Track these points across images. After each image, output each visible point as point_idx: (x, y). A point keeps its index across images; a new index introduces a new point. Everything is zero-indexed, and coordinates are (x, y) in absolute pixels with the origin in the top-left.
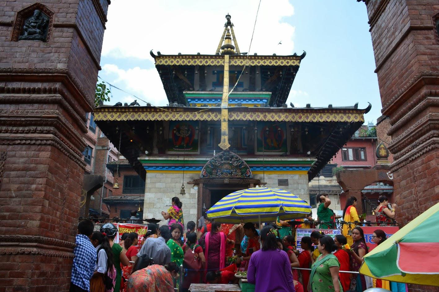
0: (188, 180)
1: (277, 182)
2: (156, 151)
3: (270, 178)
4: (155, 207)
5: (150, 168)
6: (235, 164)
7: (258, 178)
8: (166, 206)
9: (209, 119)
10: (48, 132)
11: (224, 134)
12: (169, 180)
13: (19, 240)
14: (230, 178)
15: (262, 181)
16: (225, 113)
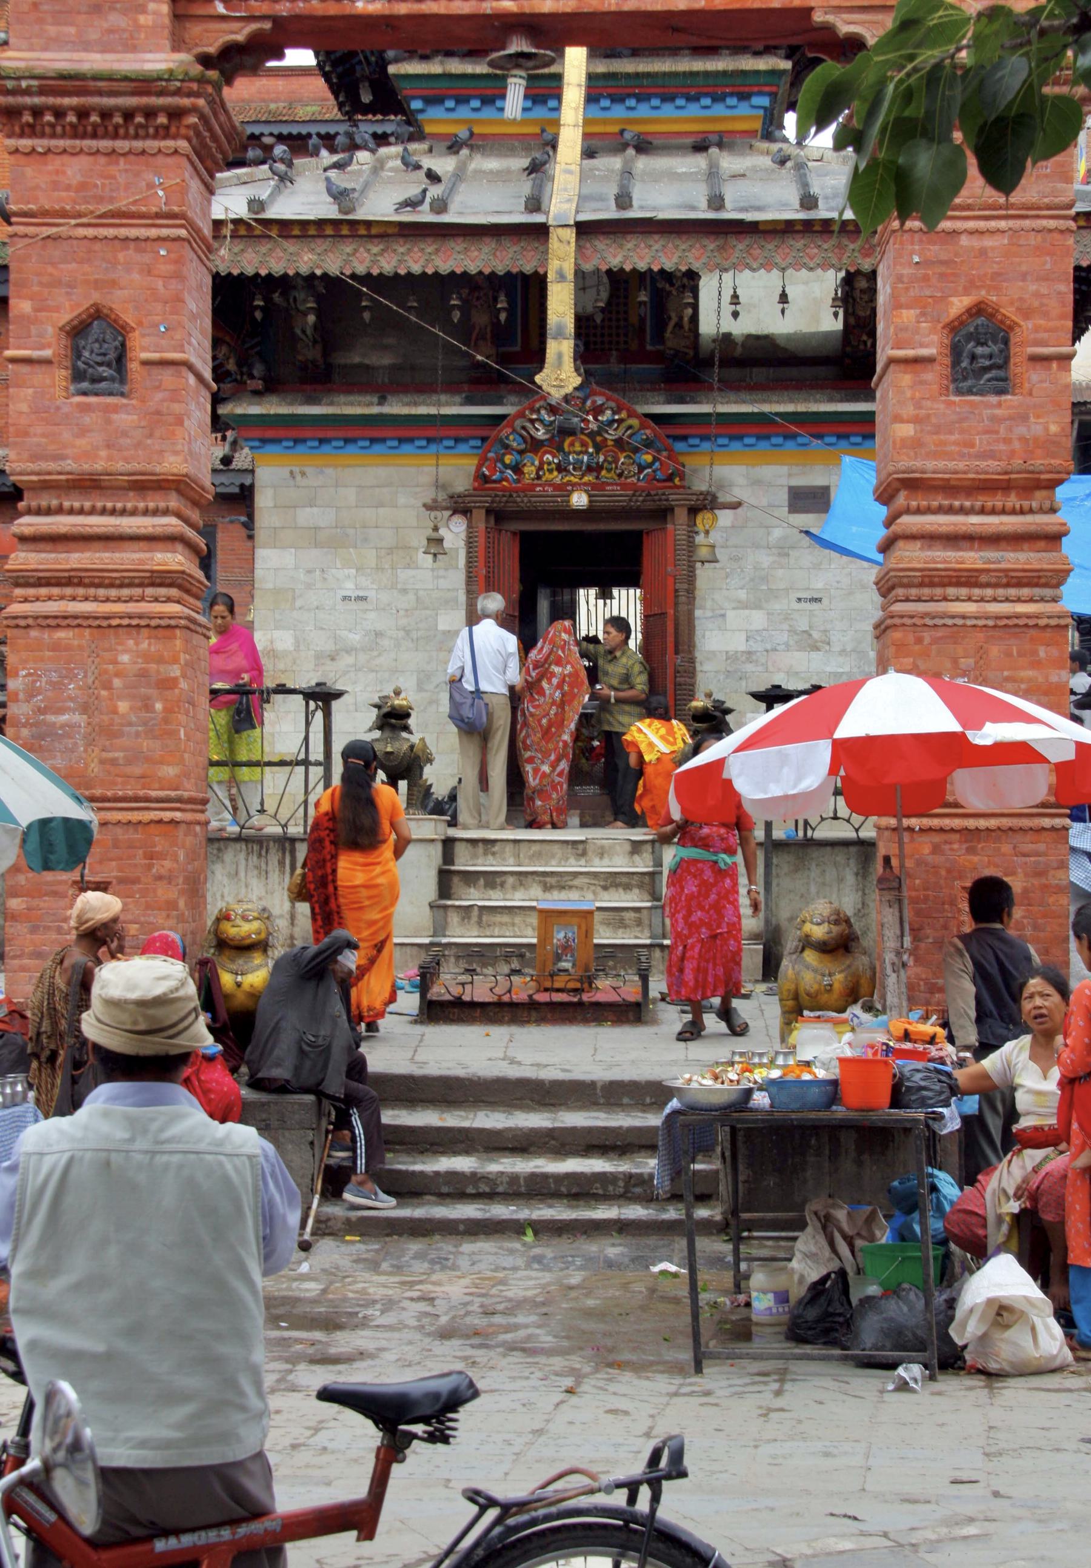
0: (428, 496)
1: (783, 497)
3: (757, 483)
4: (298, 604)
5: (271, 448)
7: (700, 485)
8: (345, 598)
10: (169, 600)
12: (350, 495)
13: (147, 799)
14: (594, 487)
15: (723, 498)
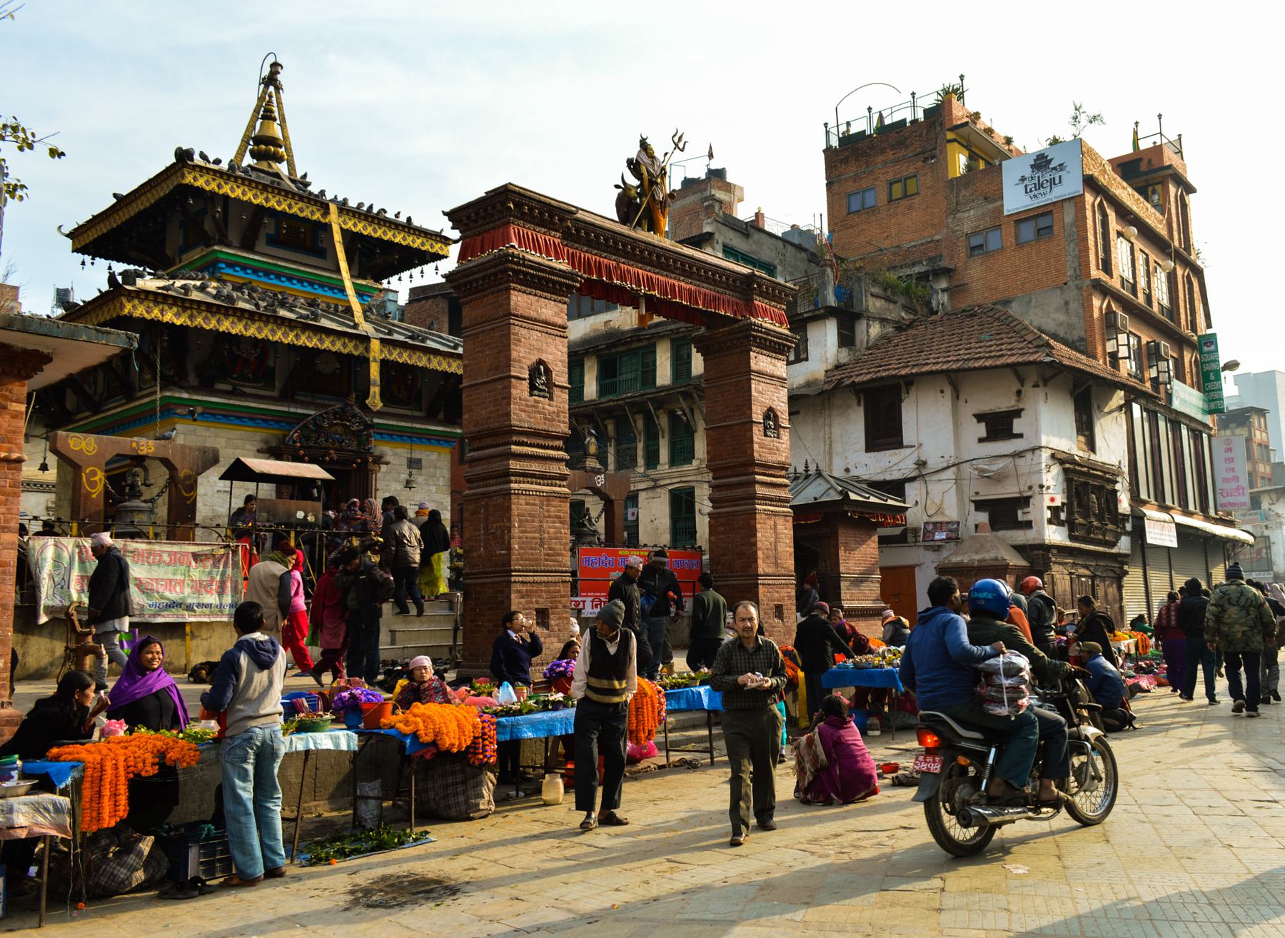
0: (259, 446)
1: (405, 461)
2: (193, 380)
3: (395, 454)
6: (355, 428)
9: (345, 351)
11: (375, 385)
16: (375, 345)
